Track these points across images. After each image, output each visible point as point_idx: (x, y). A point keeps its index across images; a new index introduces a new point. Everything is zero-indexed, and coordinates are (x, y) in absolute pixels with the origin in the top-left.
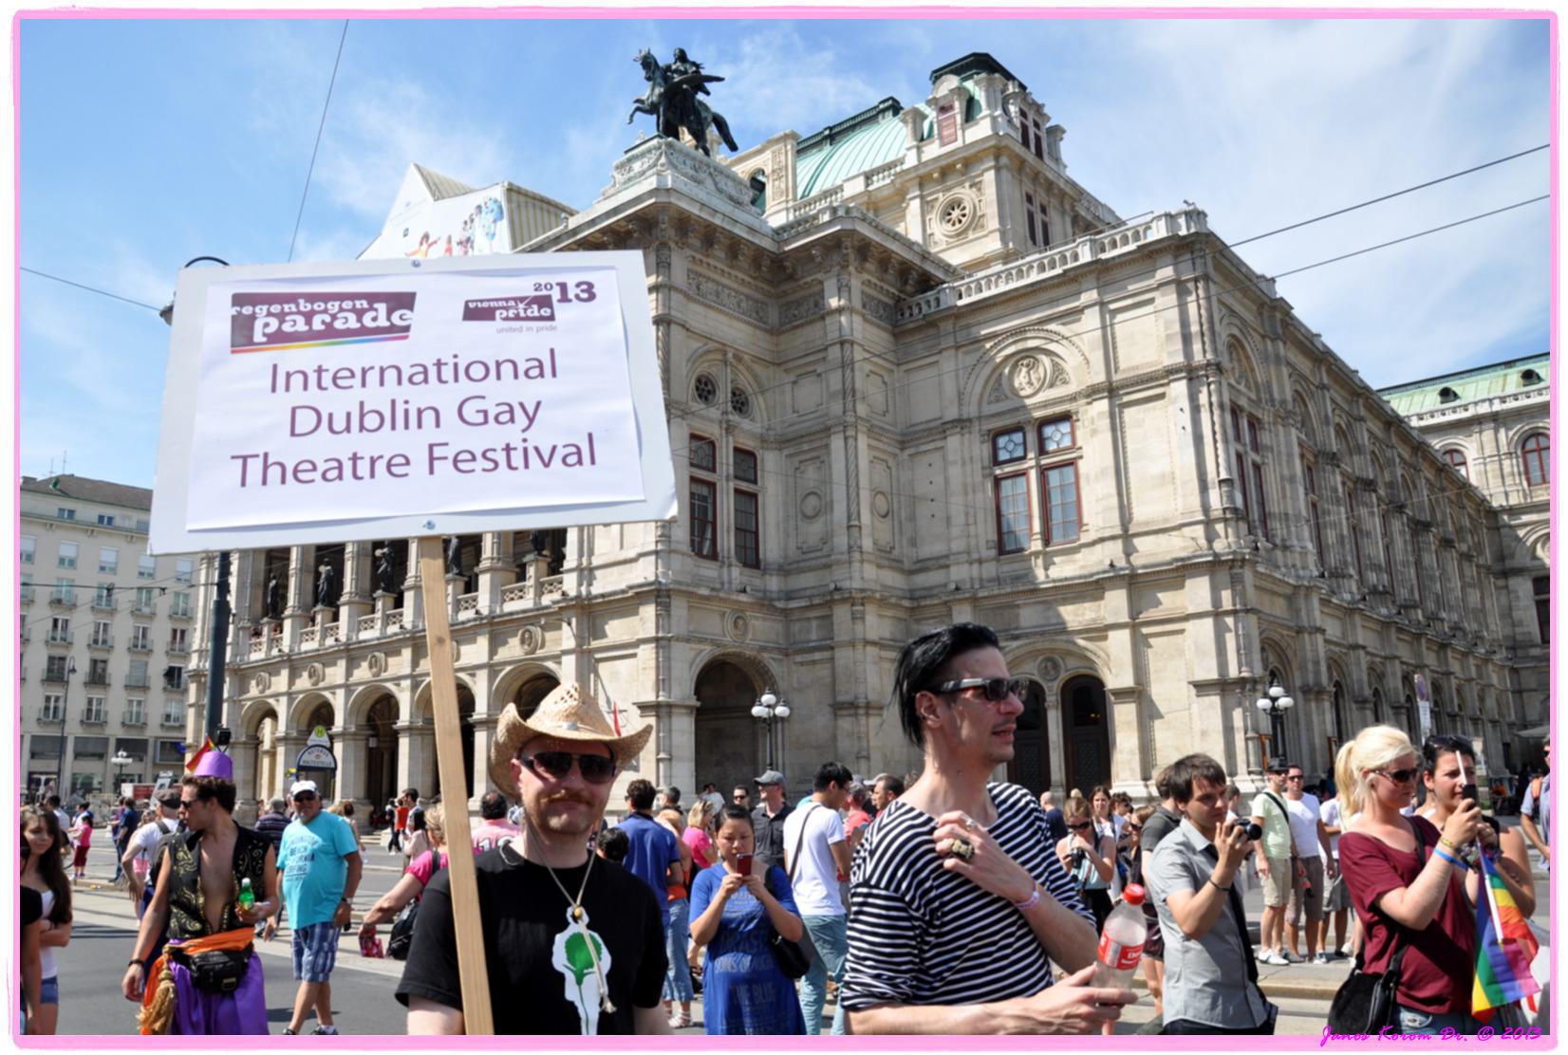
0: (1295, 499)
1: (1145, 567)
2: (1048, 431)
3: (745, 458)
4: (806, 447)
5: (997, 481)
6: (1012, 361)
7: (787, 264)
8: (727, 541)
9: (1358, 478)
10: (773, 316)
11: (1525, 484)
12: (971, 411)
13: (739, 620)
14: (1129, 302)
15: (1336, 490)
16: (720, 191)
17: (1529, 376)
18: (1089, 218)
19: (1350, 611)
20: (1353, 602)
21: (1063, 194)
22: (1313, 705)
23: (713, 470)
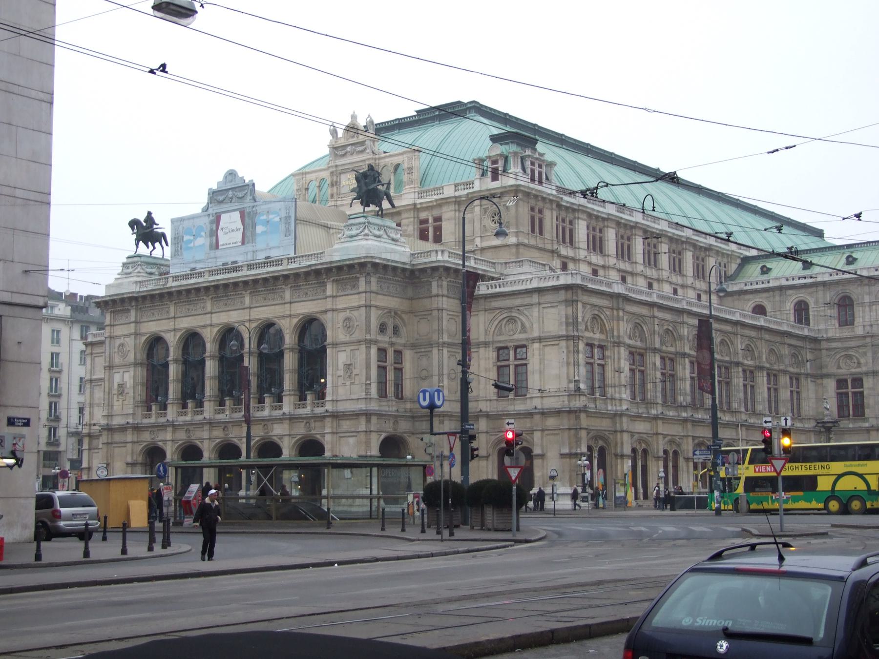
0: (619, 377)
1: (547, 409)
2: (519, 350)
3: (398, 353)
4: (423, 350)
5: (499, 367)
6: (506, 320)
7: (417, 273)
8: (390, 390)
9: (676, 354)
10: (410, 292)
11: (837, 325)
12: (490, 338)
13: (396, 422)
14: (549, 305)
15: (655, 364)
16: (389, 236)
17: (851, 260)
18: (568, 205)
19: (656, 418)
20: (658, 415)
21: (551, 201)
22: (619, 461)
23: (386, 362)
